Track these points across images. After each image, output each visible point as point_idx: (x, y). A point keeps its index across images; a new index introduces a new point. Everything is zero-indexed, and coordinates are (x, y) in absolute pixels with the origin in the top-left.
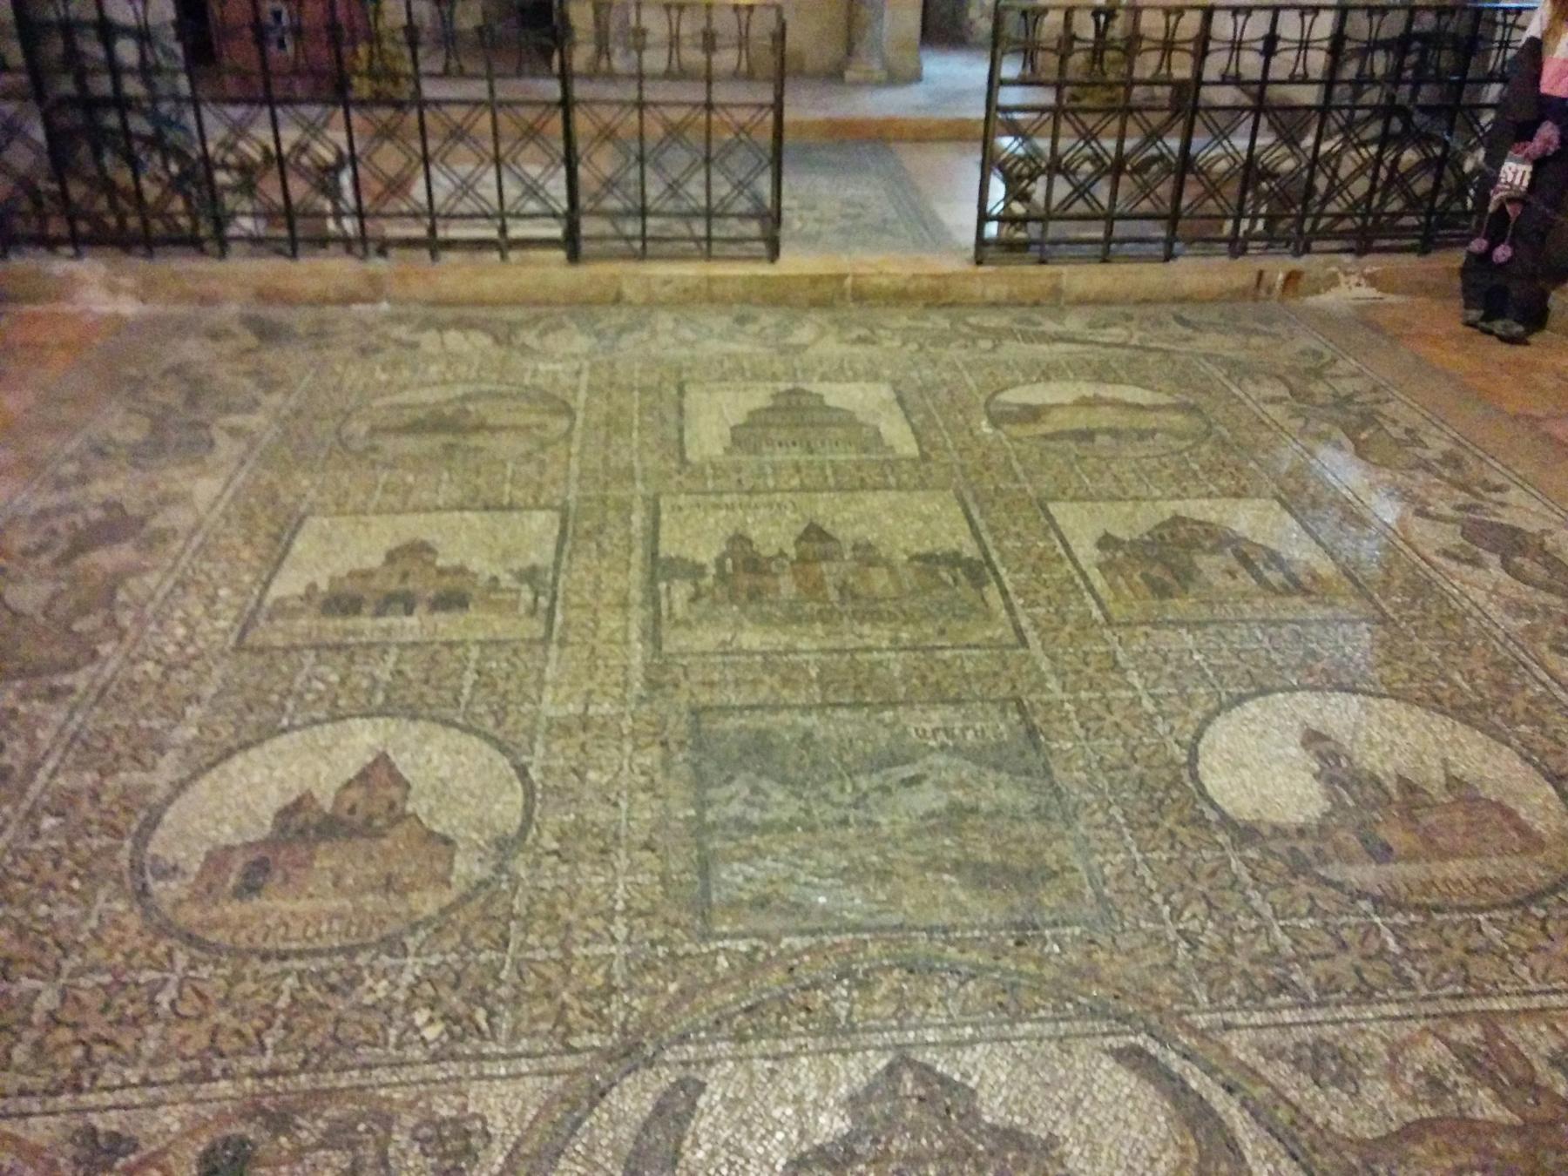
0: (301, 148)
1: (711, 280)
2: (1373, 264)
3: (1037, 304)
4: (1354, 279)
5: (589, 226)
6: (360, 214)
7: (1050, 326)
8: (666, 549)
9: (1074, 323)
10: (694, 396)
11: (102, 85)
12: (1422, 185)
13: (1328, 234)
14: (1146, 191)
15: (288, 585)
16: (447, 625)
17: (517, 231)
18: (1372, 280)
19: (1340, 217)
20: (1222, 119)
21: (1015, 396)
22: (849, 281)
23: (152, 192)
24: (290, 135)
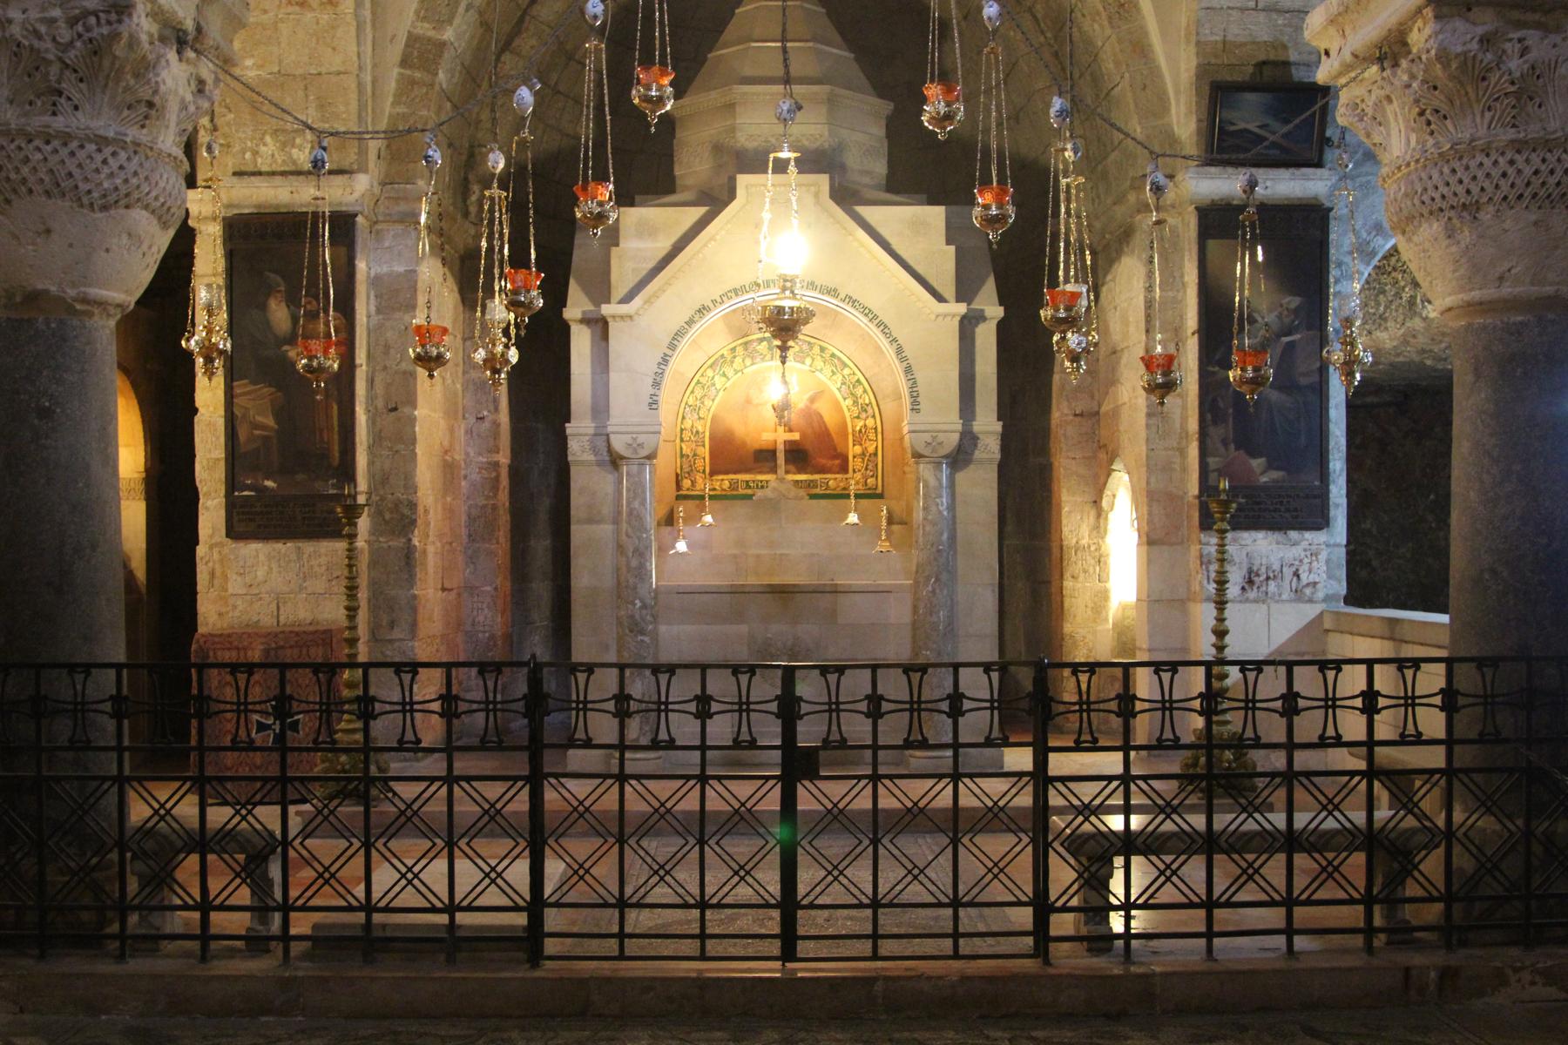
4: (1526, 976)
5: (553, 920)
20: (1329, 786)
22: (879, 987)
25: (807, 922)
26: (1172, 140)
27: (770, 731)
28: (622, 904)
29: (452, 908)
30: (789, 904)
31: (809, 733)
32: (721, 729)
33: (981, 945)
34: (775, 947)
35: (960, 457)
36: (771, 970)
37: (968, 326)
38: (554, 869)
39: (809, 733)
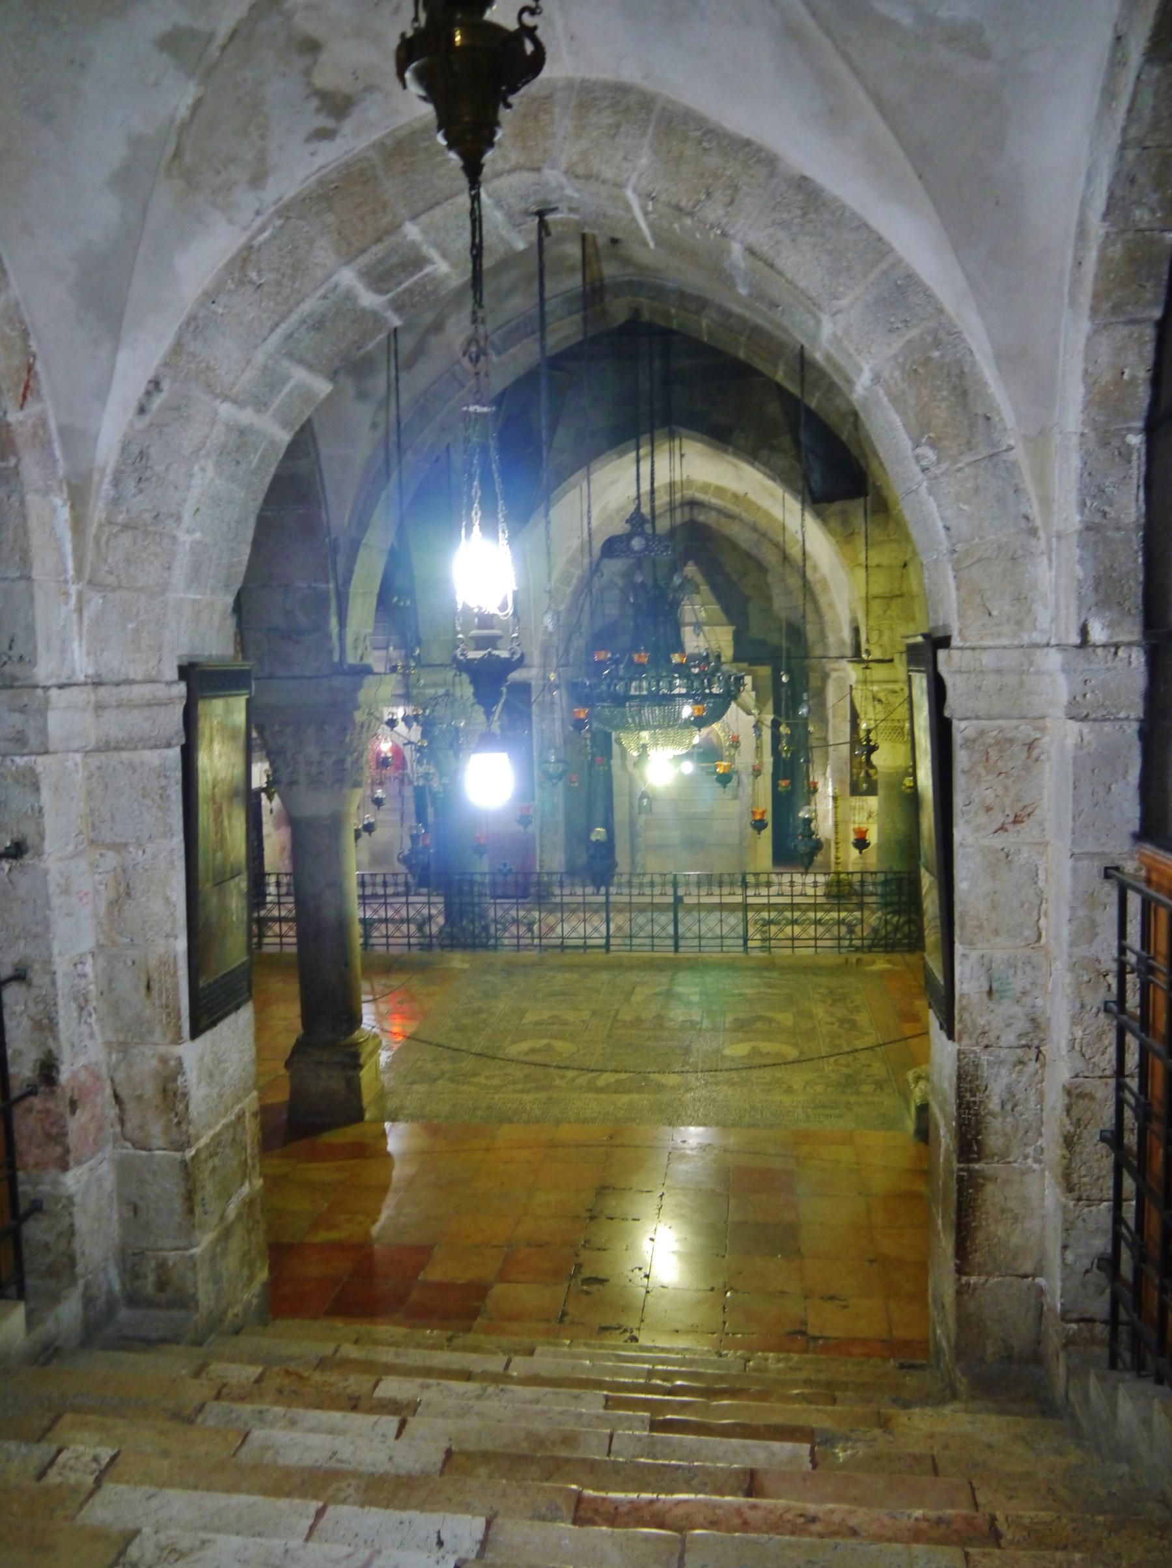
0: (502, 917)
1: (653, 959)
2: (888, 957)
3: (767, 969)
5: (612, 941)
6: (540, 938)
7: (766, 974)
8: (619, 1017)
9: (775, 974)
10: (637, 989)
11: (466, 899)
12: (906, 929)
13: (877, 946)
14: (804, 931)
15: (524, 1021)
16: (562, 1027)
17: (590, 942)
18: (889, 962)
19: (881, 940)
21: (737, 991)
23: (477, 931)
24: (522, 913)
25: (682, 943)
26: (843, 643)
27: (670, 890)
28: (631, 937)
29: (585, 938)
30: (676, 937)
31: (680, 892)
32: (657, 890)
33: (732, 949)
34: (672, 949)
35: (757, 772)
36: (671, 955)
37: (757, 727)
38: (612, 926)
39: (680, 892)
